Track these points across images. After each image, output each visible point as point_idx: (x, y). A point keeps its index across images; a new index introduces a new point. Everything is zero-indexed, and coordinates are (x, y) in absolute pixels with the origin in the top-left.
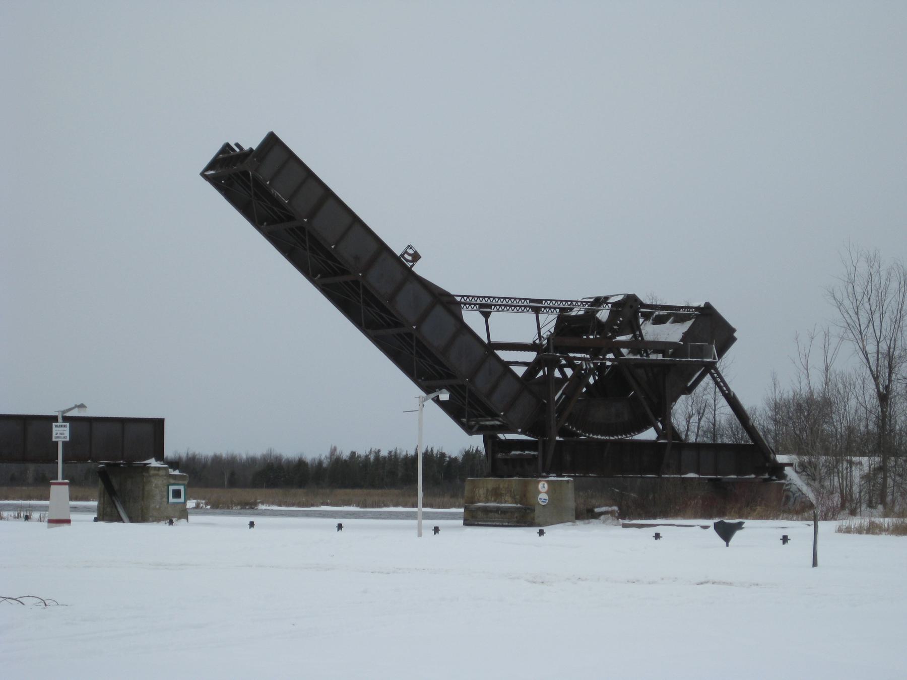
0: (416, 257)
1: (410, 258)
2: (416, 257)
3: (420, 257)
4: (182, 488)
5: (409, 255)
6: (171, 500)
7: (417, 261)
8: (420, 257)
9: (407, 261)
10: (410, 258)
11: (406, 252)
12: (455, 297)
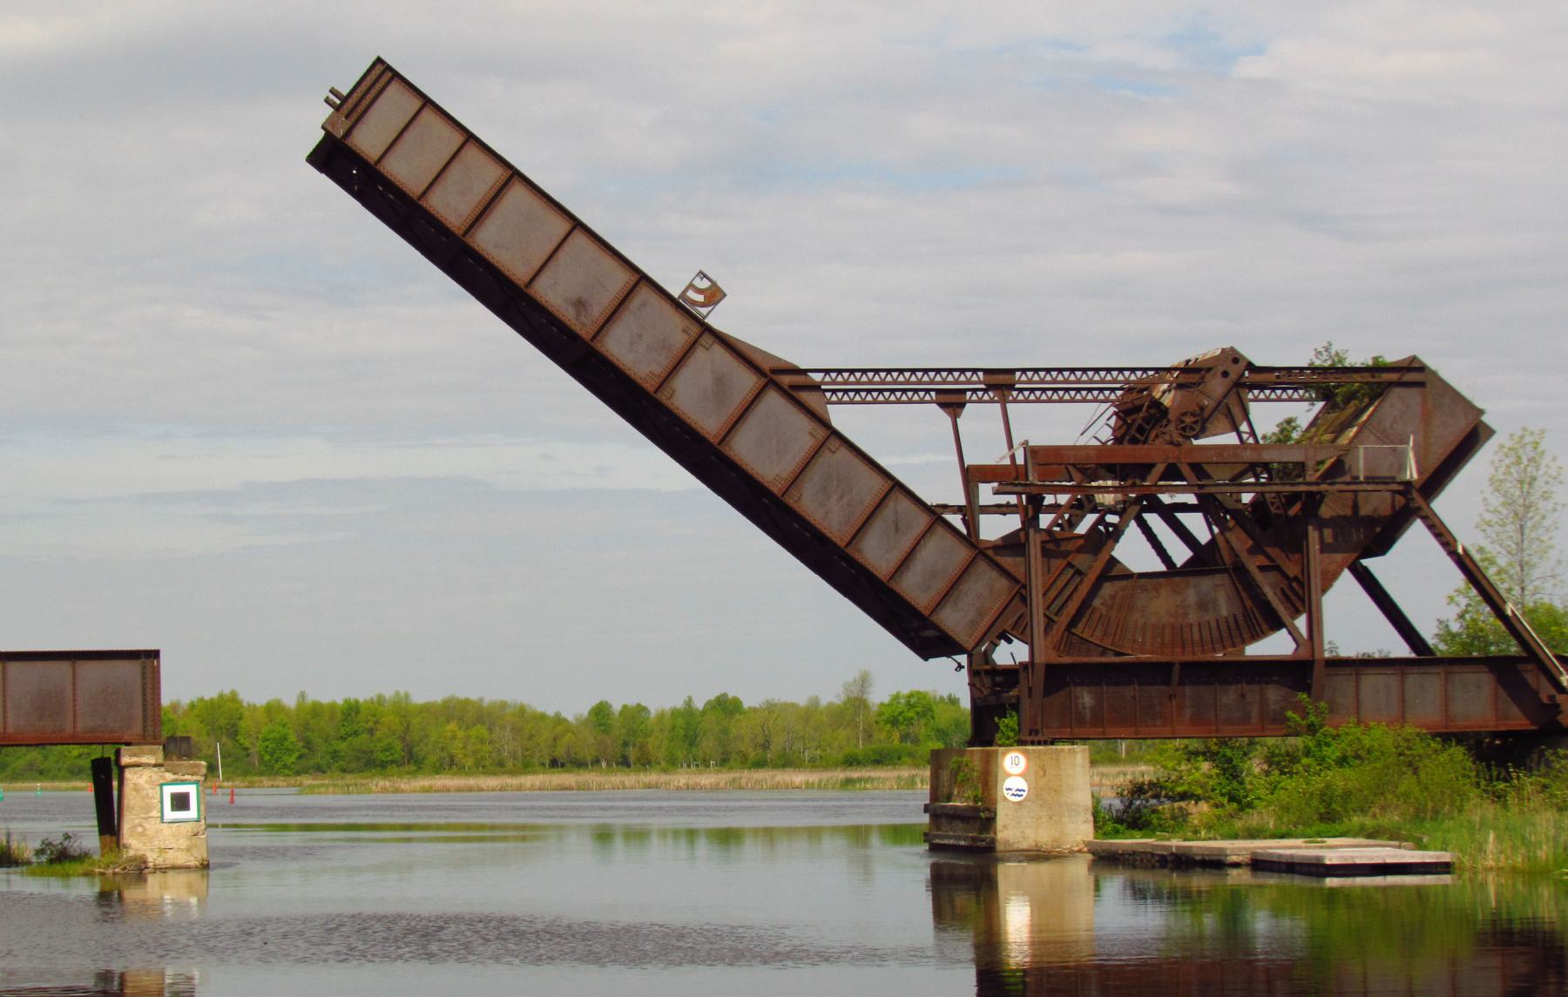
0: (714, 295)
1: (700, 298)
2: (714, 295)
3: (724, 295)
4: (192, 790)
5: (700, 291)
6: (170, 815)
7: (716, 303)
8: (724, 295)
9: (694, 303)
10: (700, 298)
11: (691, 286)
12: (810, 374)
